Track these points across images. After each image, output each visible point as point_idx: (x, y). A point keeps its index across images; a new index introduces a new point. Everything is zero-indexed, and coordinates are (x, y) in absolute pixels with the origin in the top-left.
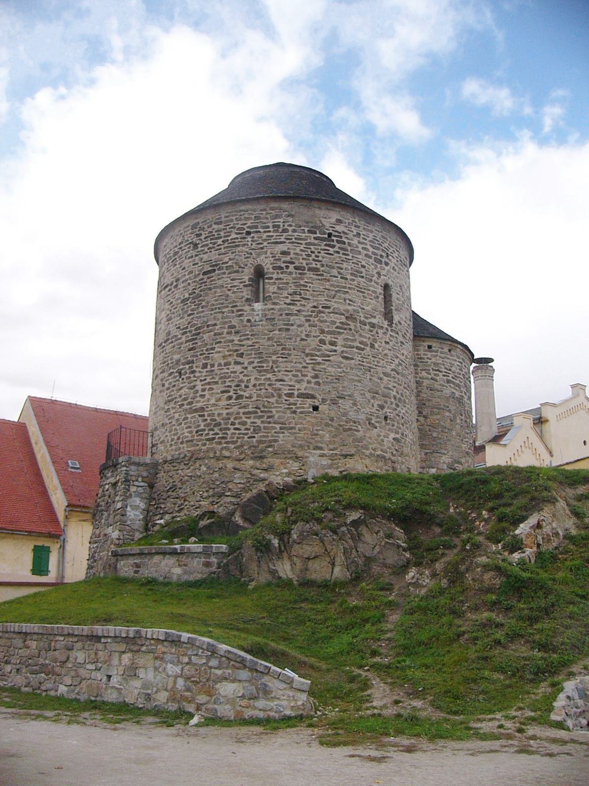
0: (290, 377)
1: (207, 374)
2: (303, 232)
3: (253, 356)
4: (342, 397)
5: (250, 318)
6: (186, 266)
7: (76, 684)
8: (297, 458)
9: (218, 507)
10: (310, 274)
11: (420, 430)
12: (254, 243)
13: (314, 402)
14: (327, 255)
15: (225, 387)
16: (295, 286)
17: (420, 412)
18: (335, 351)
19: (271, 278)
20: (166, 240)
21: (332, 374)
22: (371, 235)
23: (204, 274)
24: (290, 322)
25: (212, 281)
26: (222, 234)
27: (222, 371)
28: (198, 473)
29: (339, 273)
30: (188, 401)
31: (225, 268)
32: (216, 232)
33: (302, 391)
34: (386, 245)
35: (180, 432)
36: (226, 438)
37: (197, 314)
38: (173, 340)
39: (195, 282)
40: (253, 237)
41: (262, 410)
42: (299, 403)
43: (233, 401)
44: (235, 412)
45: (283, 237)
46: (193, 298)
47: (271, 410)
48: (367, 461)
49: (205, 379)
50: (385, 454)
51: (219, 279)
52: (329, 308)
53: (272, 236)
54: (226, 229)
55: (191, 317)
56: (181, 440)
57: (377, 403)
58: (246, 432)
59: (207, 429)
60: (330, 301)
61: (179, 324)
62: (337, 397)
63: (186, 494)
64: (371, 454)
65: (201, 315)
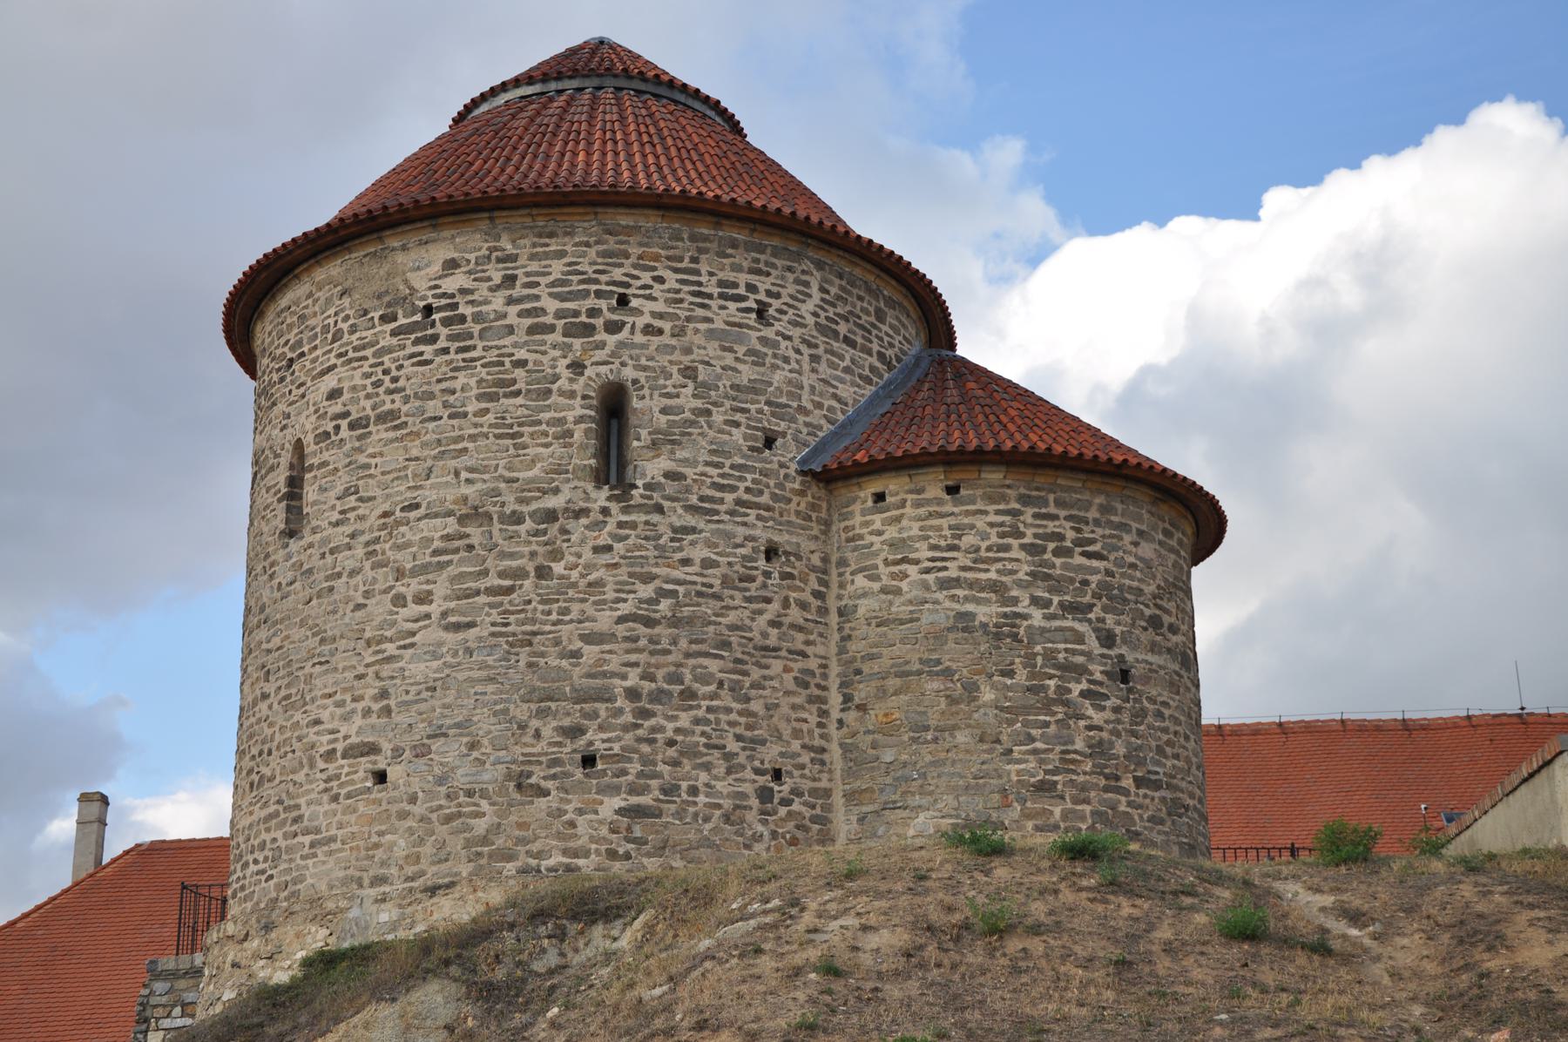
0: (332, 708)
2: (370, 324)
4: (440, 734)
10: (379, 433)
13: (375, 763)
14: (416, 369)
17: (847, 699)
18: (428, 616)
19: (311, 468)
21: (419, 678)
22: (557, 268)
33: (354, 740)
34: (617, 274)
42: (346, 770)
45: (334, 354)
47: (298, 801)
50: (581, 862)
52: (417, 506)
57: (554, 724)
62: (429, 737)
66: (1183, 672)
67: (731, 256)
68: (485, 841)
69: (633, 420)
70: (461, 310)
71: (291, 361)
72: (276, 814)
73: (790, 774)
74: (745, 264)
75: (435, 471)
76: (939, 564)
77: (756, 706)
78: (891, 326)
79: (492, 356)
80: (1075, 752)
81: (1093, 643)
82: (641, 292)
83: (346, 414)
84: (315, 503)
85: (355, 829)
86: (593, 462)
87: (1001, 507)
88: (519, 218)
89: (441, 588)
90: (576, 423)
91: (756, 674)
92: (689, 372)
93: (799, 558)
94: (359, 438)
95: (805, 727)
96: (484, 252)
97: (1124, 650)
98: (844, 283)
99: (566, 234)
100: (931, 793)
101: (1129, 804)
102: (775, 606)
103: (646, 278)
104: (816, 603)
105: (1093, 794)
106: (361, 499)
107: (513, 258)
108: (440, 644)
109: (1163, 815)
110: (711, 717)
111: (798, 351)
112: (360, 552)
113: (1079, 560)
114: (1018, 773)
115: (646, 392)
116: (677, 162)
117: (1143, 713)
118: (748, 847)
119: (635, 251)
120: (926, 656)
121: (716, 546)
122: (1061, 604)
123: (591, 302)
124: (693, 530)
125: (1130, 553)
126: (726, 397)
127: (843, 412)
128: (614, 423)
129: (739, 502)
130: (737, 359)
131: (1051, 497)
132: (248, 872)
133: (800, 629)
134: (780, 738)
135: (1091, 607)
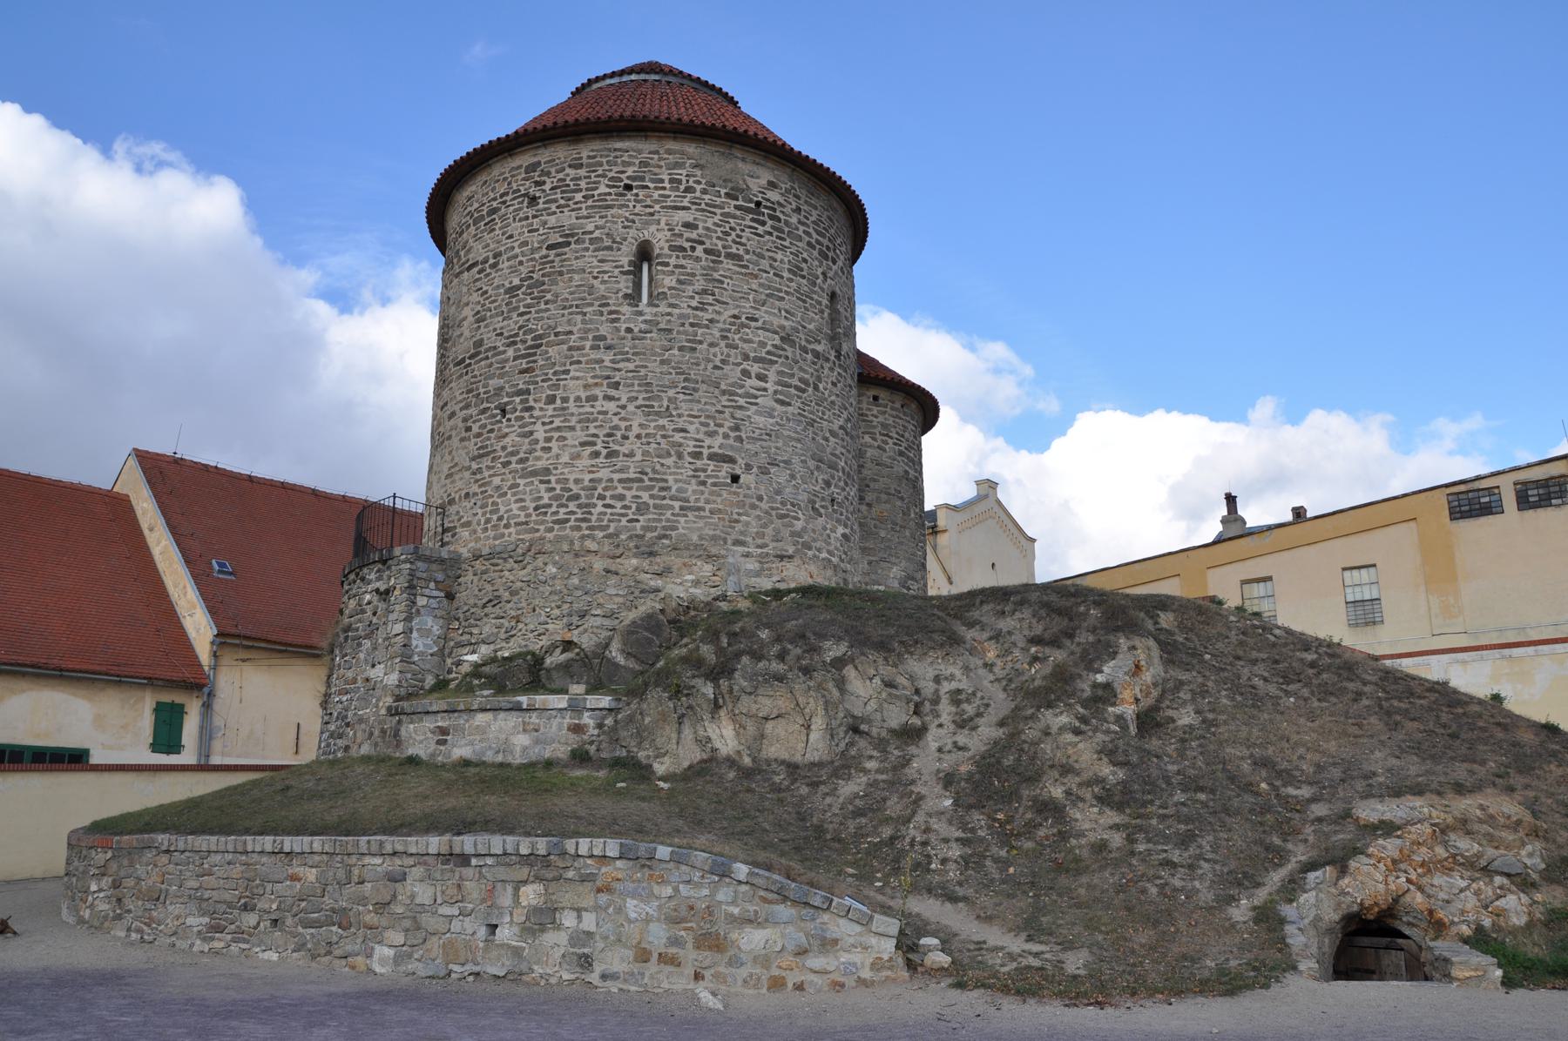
0: (698, 425)
1: (556, 413)
3: (636, 388)
5: (632, 326)
6: (516, 233)
7: (415, 942)
8: (709, 557)
9: (581, 634)
10: (728, 264)
11: (861, 525)
12: (638, 205)
13: (734, 469)
15: (587, 436)
16: (705, 280)
17: (861, 499)
18: (765, 390)
19: (667, 264)
20: (473, 188)
21: (761, 426)
22: (814, 213)
23: (550, 247)
24: (698, 338)
25: (565, 260)
26: (583, 184)
27: (581, 410)
28: (541, 578)
29: (771, 266)
30: (519, 457)
31: (587, 241)
32: (571, 180)
33: (716, 450)
35: (502, 509)
36: (589, 520)
37: (537, 312)
38: (490, 354)
39: (532, 260)
40: (637, 195)
41: (651, 475)
42: (711, 468)
43: (601, 459)
44: (605, 479)
45: (687, 199)
46: (529, 287)
47: (664, 477)
48: (812, 568)
49: (552, 422)
51: (577, 258)
52: (756, 320)
53: (669, 196)
54: (590, 177)
55: (526, 317)
56: (505, 521)
58: (623, 511)
59: (555, 504)
60: (758, 309)
61: (502, 328)
63: (520, 612)
64: (815, 556)
65: (545, 315)
75: (768, 304)
85: (720, 507)
89: (772, 376)
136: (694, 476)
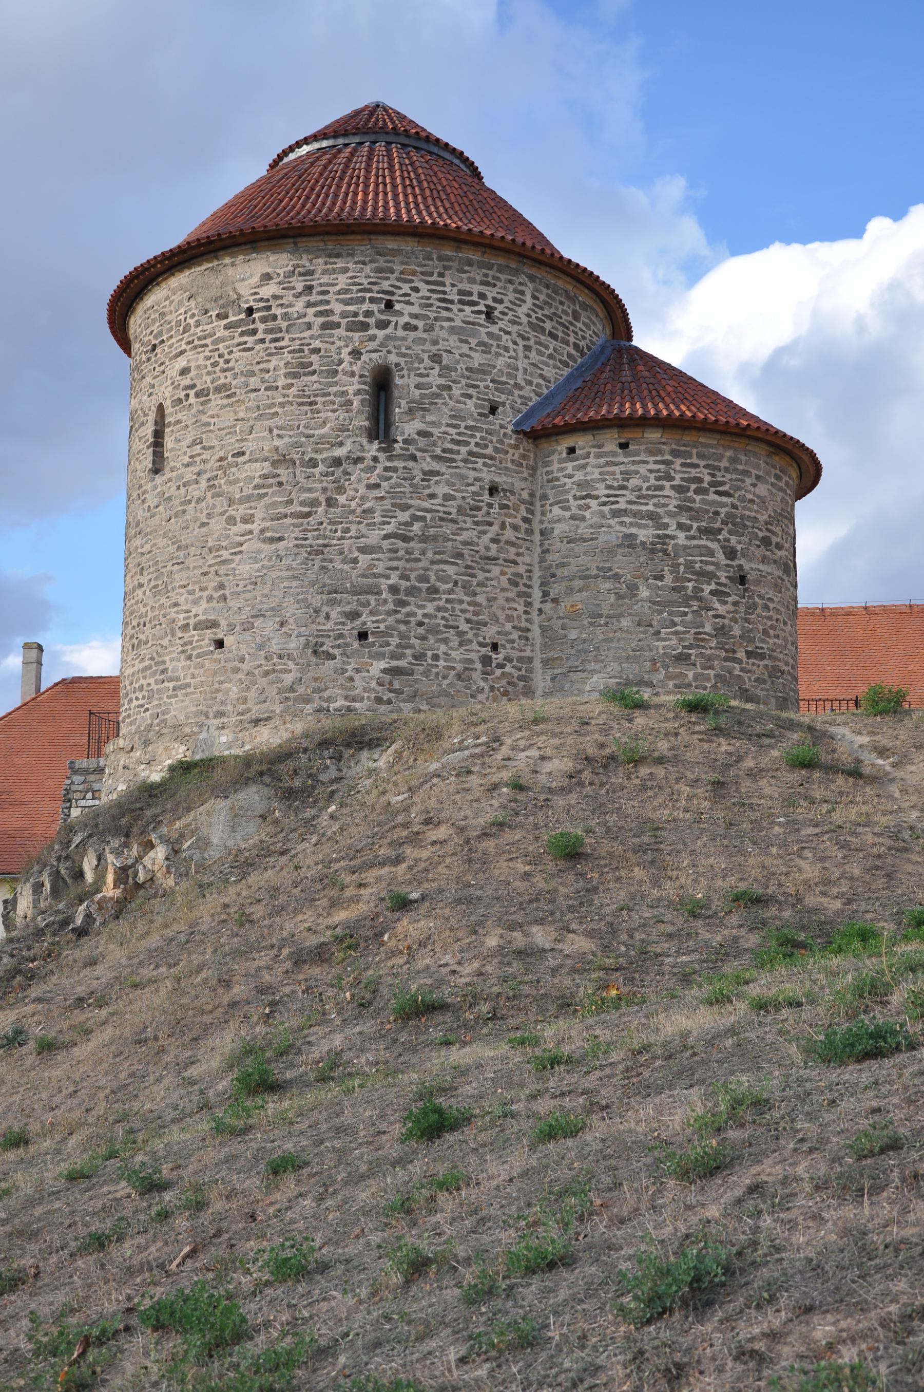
0: (185, 595)
10: (217, 400)
17: (545, 594)
18: (251, 532)
22: (342, 281)
33: (202, 617)
34: (385, 285)
42: (196, 638)
50: (357, 705)
52: (243, 454)
57: (339, 609)
62: (253, 617)
66: (785, 577)
67: (466, 272)
68: (292, 689)
69: (396, 393)
70: (273, 311)
71: (155, 346)
72: (150, 667)
73: (504, 646)
74: (478, 278)
76: (612, 499)
77: (480, 599)
78: (584, 324)
79: (296, 345)
80: (705, 633)
81: (720, 557)
82: (402, 299)
83: (193, 386)
84: (173, 449)
85: (203, 679)
86: (366, 423)
87: (658, 458)
88: (315, 243)
89: (259, 514)
90: (355, 395)
91: (481, 576)
92: (436, 358)
93: (513, 493)
94: (203, 404)
95: (515, 614)
96: (290, 268)
97: (742, 562)
98: (550, 292)
99: (349, 255)
100: (602, 661)
101: (742, 670)
102: (495, 528)
103: (406, 288)
104: (524, 526)
105: (716, 663)
106: (204, 448)
107: (311, 273)
108: (259, 552)
109: (766, 677)
110: (449, 606)
111: (515, 343)
112: (203, 484)
113: (713, 497)
114: (664, 647)
115: (405, 372)
116: (430, 201)
117: (754, 606)
118: (473, 696)
119: (398, 268)
120: (601, 565)
121: (454, 485)
122: (699, 528)
123: (365, 307)
124: (438, 473)
125: (750, 492)
126: (463, 376)
127: (547, 387)
128: (383, 394)
129: (470, 453)
130: (471, 348)
131: (695, 451)
132: (133, 705)
133: (513, 544)
134: (497, 621)
135: (720, 531)
136: (183, 652)
